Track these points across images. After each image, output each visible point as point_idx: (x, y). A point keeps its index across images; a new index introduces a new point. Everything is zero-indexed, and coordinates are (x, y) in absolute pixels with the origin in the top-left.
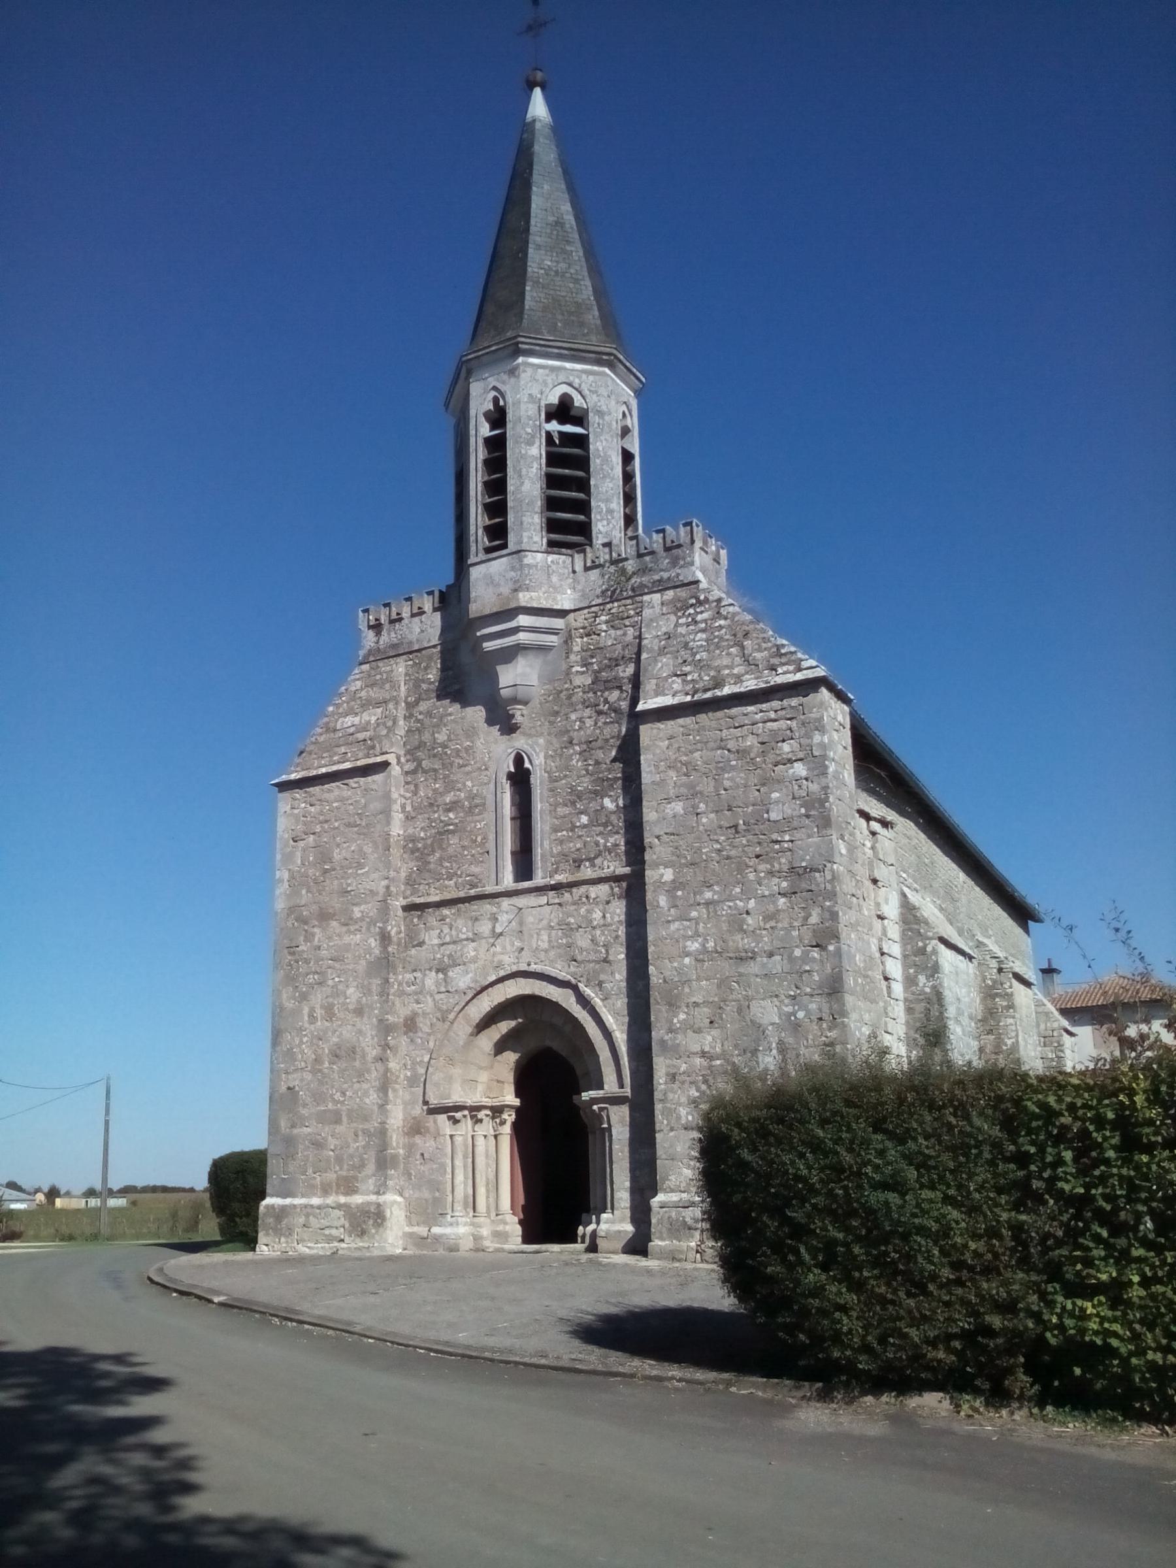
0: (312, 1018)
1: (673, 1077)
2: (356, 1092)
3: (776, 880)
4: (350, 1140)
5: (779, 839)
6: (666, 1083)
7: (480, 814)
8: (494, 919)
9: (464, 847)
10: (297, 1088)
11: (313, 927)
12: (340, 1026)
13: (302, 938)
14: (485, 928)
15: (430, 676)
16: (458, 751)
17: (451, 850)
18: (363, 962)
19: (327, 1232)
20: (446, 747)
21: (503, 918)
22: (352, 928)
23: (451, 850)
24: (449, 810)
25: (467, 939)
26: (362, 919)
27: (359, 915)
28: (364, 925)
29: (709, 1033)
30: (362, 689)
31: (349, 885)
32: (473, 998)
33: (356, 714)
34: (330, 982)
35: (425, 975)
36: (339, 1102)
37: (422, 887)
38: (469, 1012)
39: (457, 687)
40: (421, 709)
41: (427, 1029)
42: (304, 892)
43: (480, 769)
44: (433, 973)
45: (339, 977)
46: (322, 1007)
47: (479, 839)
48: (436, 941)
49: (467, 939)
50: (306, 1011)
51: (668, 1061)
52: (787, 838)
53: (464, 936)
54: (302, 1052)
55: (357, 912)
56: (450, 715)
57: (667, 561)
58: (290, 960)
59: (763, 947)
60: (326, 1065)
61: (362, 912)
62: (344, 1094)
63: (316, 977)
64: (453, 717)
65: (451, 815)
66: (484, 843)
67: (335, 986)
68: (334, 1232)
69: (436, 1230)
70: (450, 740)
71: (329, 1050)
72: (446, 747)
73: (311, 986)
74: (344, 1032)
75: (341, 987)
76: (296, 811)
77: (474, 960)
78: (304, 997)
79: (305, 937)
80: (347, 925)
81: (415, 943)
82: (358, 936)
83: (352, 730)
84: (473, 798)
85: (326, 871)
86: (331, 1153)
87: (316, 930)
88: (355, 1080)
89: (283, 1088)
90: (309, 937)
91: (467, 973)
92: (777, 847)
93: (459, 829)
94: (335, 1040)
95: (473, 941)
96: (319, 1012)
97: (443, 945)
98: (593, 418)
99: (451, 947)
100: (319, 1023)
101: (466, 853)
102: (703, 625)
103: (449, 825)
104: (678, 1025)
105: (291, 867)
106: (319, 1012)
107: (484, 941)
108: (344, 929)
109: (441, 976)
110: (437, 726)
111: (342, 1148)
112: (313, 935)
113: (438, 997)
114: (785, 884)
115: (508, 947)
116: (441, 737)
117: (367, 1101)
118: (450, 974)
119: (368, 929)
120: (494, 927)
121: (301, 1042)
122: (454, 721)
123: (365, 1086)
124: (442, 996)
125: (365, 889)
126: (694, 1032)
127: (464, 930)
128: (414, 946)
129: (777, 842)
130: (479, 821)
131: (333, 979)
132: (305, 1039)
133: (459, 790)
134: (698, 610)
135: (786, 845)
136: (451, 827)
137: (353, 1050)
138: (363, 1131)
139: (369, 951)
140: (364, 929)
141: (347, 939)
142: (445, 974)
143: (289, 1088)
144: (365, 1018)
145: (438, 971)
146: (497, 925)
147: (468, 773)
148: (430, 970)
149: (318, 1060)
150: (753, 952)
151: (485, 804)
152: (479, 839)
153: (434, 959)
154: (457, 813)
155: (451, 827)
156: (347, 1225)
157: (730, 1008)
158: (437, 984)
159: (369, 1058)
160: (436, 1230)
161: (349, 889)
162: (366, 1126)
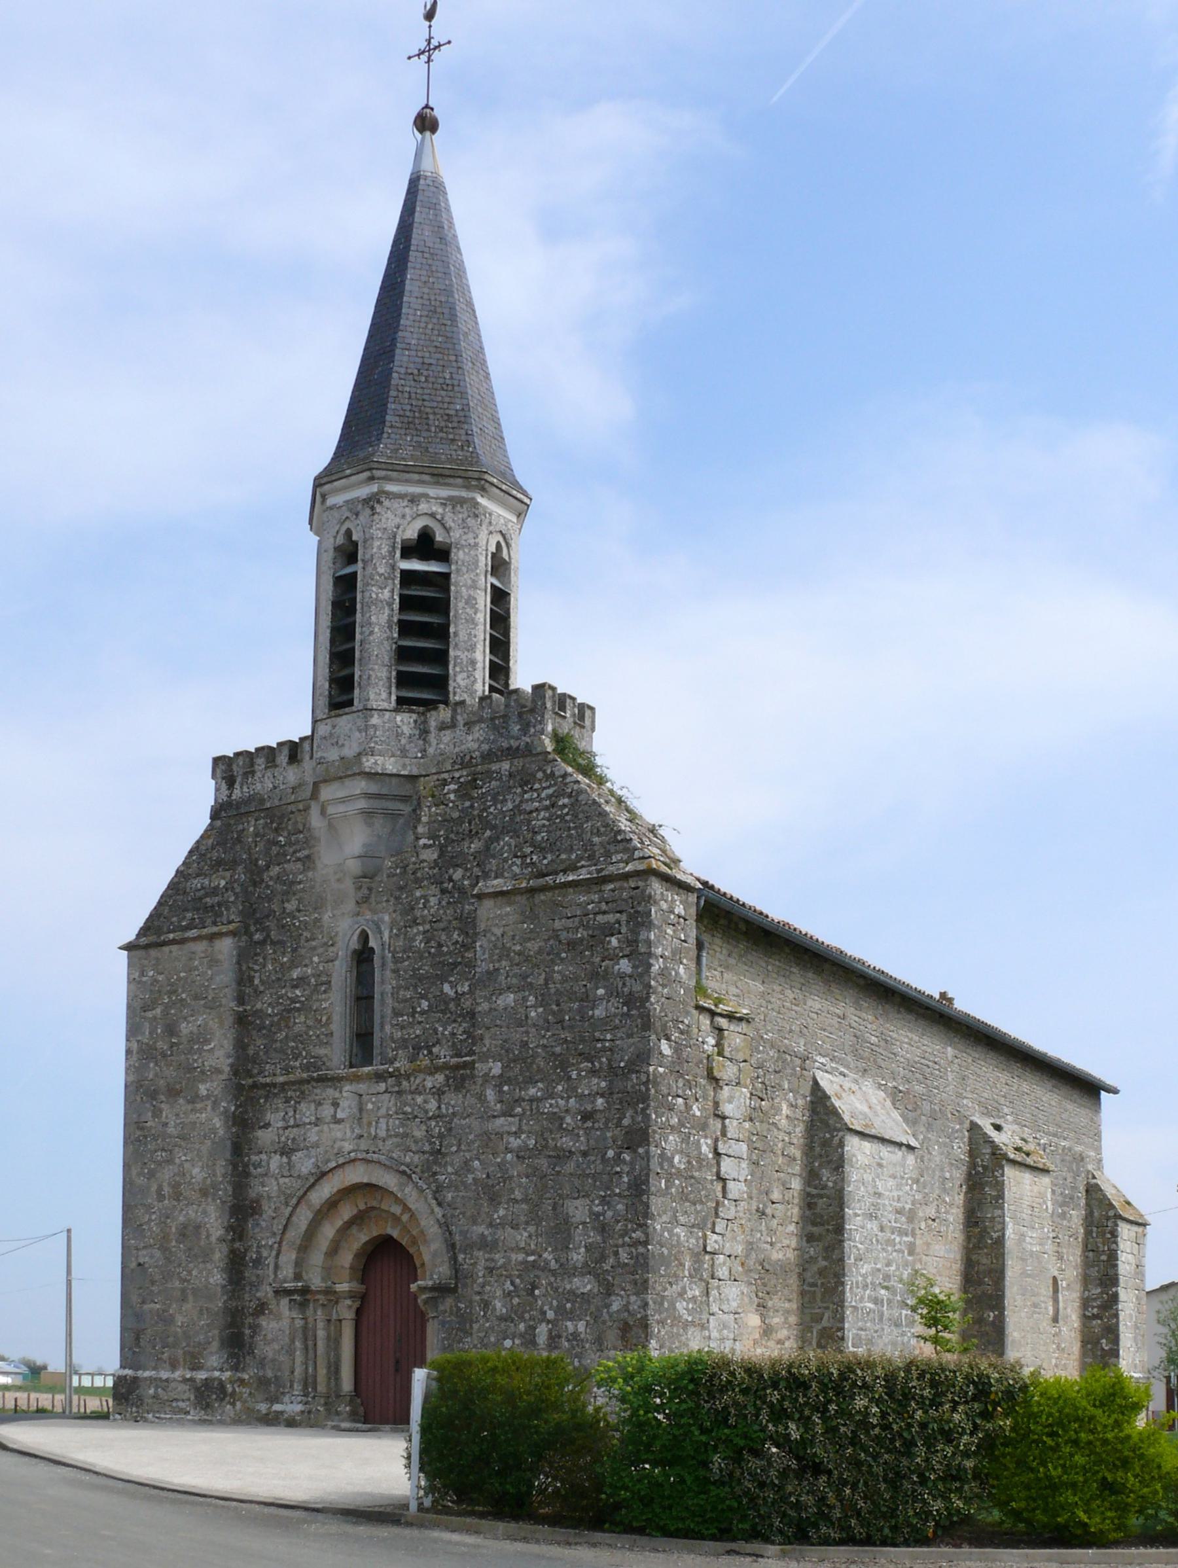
0: (160, 1197)
1: (490, 1270)
2: (200, 1272)
3: (596, 1081)
4: (195, 1318)
5: (602, 1037)
6: (484, 1276)
7: (325, 992)
8: (336, 1105)
9: (309, 1027)
10: (147, 1266)
11: (162, 1102)
12: (187, 1205)
13: (150, 1114)
14: (327, 1111)
15: (281, 839)
16: (306, 923)
17: (297, 1029)
18: (209, 1143)
19: (174, 1404)
20: (294, 917)
21: (344, 1104)
22: (198, 1106)
23: (297, 1029)
24: (296, 987)
25: (310, 1123)
26: (208, 1097)
27: (205, 1093)
28: (209, 1103)
29: (525, 1229)
30: (213, 848)
31: (195, 1061)
32: (317, 1181)
33: (206, 875)
34: (177, 1161)
35: (270, 1158)
36: (185, 1280)
37: (268, 1067)
38: (311, 1197)
39: (306, 852)
40: (271, 874)
41: (270, 1213)
42: (152, 1065)
43: (325, 944)
44: (278, 1157)
45: (185, 1155)
46: (169, 1184)
47: (324, 1019)
48: (280, 1124)
49: (310, 1123)
50: (154, 1188)
51: (487, 1256)
52: (609, 1037)
53: (307, 1121)
54: (150, 1229)
55: (203, 1089)
56: (300, 883)
57: (518, 727)
58: (139, 1136)
59: (579, 1147)
60: (174, 1243)
61: (208, 1090)
62: (190, 1273)
63: (164, 1154)
64: (302, 886)
65: (298, 992)
66: (328, 1025)
67: (181, 1165)
68: (181, 1404)
69: (277, 1407)
70: (299, 911)
71: (176, 1229)
72: (294, 917)
73: (159, 1164)
74: (190, 1212)
75: (186, 1165)
76: (144, 979)
77: (316, 1145)
78: (152, 1174)
79: (153, 1112)
80: (193, 1103)
81: (262, 1124)
82: (204, 1115)
83: (199, 894)
84: (319, 976)
85: (172, 1045)
86: (179, 1330)
87: (163, 1106)
88: (200, 1260)
89: (134, 1265)
90: (157, 1113)
91: (310, 1158)
92: (599, 1045)
93: (305, 1008)
94: (181, 1219)
95: (316, 1125)
96: (166, 1190)
97: (286, 1128)
98: (458, 555)
99: (295, 1130)
100: (166, 1202)
101: (311, 1033)
102: (548, 803)
103: (296, 1003)
104: (498, 1221)
105: (140, 1038)
106: (166, 1190)
107: (326, 1126)
108: (190, 1107)
109: (285, 1159)
110: (287, 893)
111: (188, 1326)
112: (161, 1111)
113: (282, 1181)
114: (603, 1084)
115: (349, 1134)
116: (290, 906)
117: (211, 1280)
118: (294, 1158)
119: (213, 1109)
120: (335, 1112)
121: (150, 1220)
122: (303, 890)
123: (208, 1266)
124: (287, 1180)
125: (211, 1066)
126: (512, 1228)
127: (308, 1113)
128: (260, 1128)
129: (598, 1040)
130: (324, 1000)
131: (180, 1157)
132: (154, 1217)
133: (306, 966)
134: (544, 785)
135: (607, 1044)
136: (298, 1005)
137: (198, 1227)
138: (207, 1309)
139: (214, 1131)
140: (209, 1108)
141: (192, 1117)
142: (289, 1158)
143: (140, 1265)
144: (210, 1200)
145: (282, 1154)
146: (338, 1110)
147: (314, 948)
148: (275, 1152)
149: (166, 1237)
150: (570, 1152)
151: (330, 982)
152: (324, 1019)
153: (279, 1143)
154: (304, 990)
155: (298, 1005)
156: (192, 1398)
157: (547, 1206)
158: (281, 1167)
159: (213, 1239)
160: (277, 1407)
161: (196, 1065)
162: (211, 1306)
